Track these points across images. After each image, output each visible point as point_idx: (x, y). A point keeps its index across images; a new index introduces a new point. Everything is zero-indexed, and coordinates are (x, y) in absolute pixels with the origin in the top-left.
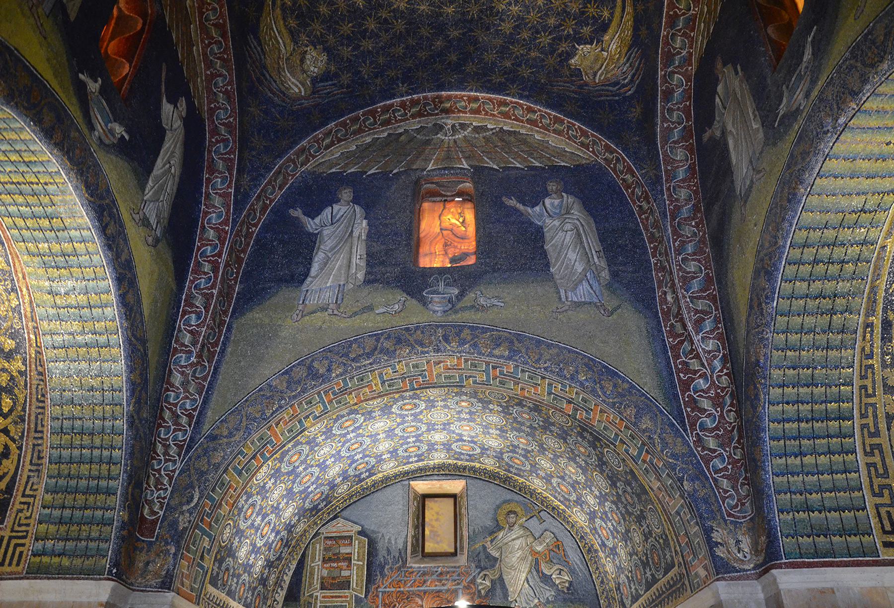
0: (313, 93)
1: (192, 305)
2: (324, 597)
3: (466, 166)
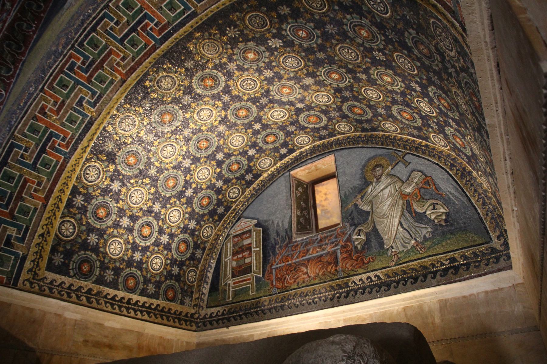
2: (234, 283)
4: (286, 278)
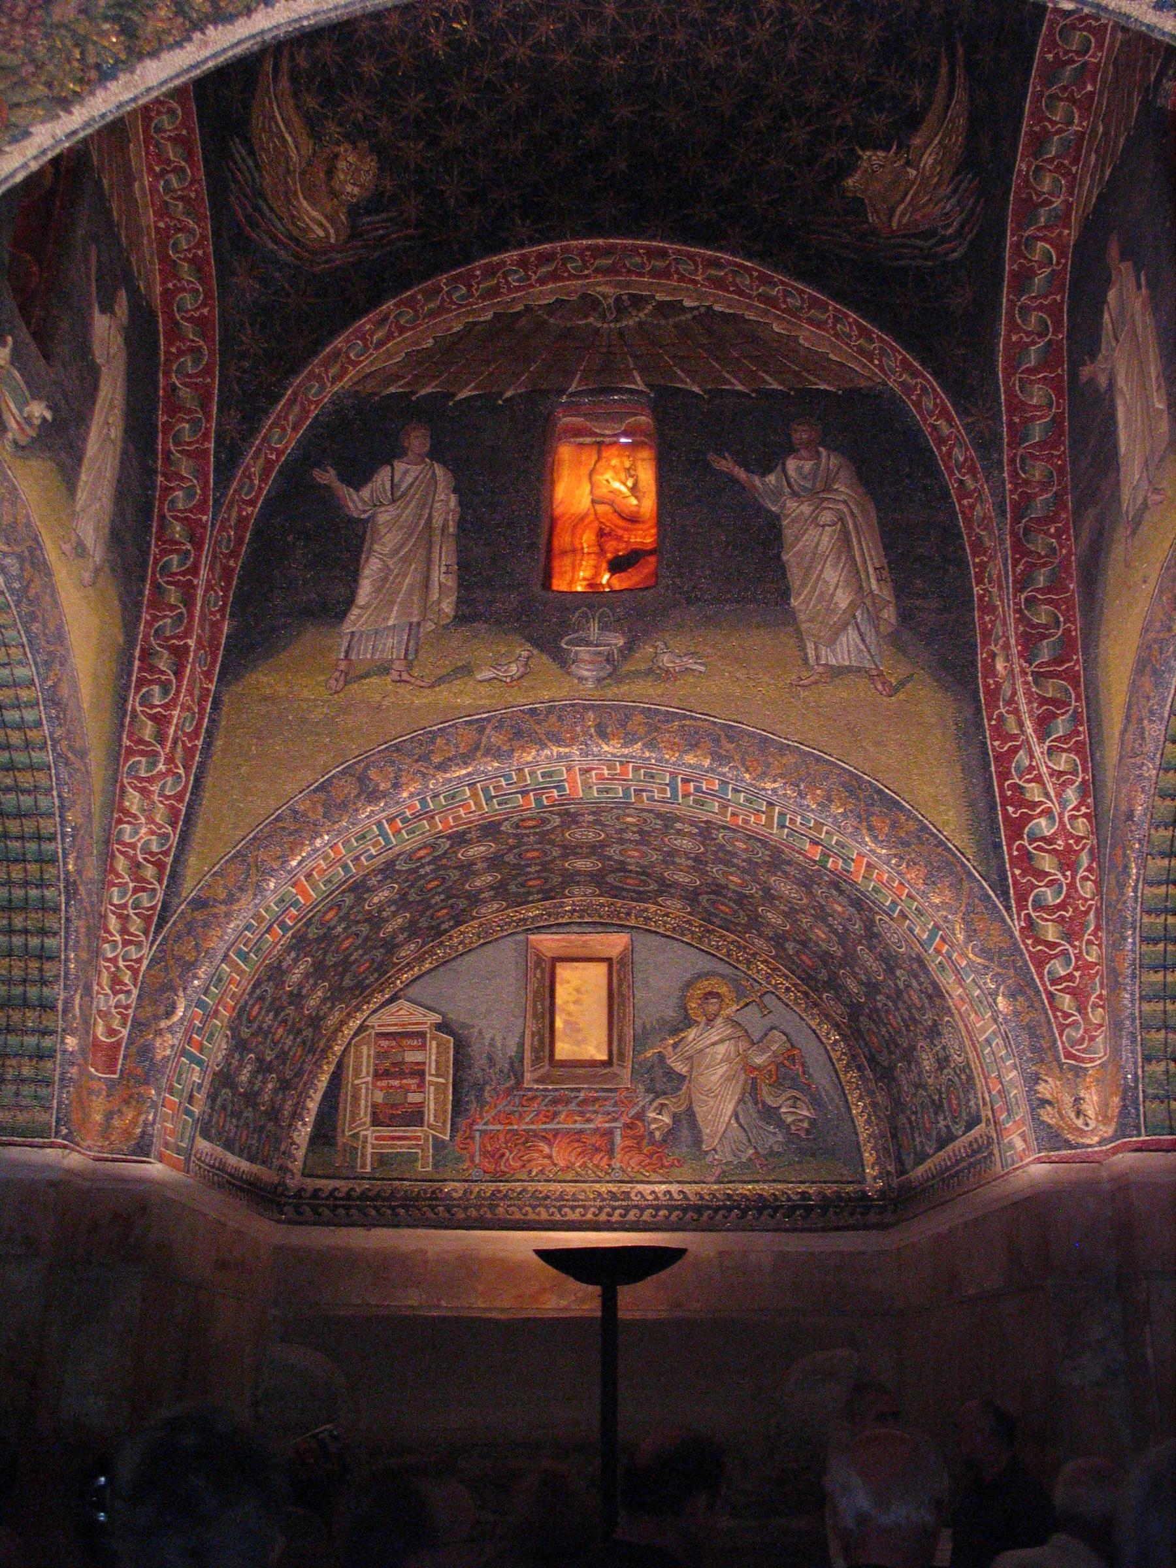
0: (352, 237)
1: (152, 669)
2: (377, 1138)
3: (642, 387)
4: (503, 1155)
